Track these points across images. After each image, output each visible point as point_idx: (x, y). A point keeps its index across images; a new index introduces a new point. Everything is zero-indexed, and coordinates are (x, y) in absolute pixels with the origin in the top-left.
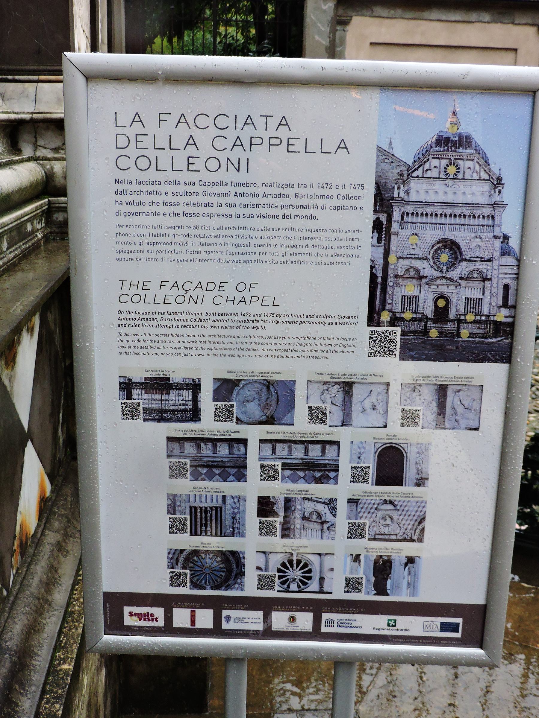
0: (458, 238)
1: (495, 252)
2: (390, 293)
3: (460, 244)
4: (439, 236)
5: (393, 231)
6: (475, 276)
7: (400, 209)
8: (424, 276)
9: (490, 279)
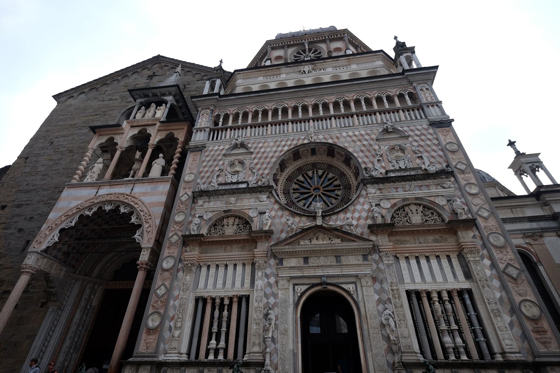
0: (342, 140)
1: (450, 156)
2: (161, 291)
3: (350, 150)
4: (295, 142)
5: (192, 144)
6: (416, 219)
7: (212, 111)
8: (261, 231)
9: (471, 223)
